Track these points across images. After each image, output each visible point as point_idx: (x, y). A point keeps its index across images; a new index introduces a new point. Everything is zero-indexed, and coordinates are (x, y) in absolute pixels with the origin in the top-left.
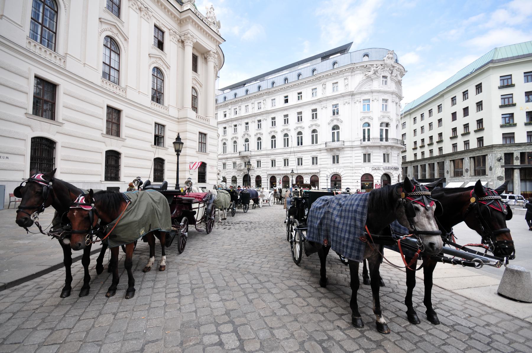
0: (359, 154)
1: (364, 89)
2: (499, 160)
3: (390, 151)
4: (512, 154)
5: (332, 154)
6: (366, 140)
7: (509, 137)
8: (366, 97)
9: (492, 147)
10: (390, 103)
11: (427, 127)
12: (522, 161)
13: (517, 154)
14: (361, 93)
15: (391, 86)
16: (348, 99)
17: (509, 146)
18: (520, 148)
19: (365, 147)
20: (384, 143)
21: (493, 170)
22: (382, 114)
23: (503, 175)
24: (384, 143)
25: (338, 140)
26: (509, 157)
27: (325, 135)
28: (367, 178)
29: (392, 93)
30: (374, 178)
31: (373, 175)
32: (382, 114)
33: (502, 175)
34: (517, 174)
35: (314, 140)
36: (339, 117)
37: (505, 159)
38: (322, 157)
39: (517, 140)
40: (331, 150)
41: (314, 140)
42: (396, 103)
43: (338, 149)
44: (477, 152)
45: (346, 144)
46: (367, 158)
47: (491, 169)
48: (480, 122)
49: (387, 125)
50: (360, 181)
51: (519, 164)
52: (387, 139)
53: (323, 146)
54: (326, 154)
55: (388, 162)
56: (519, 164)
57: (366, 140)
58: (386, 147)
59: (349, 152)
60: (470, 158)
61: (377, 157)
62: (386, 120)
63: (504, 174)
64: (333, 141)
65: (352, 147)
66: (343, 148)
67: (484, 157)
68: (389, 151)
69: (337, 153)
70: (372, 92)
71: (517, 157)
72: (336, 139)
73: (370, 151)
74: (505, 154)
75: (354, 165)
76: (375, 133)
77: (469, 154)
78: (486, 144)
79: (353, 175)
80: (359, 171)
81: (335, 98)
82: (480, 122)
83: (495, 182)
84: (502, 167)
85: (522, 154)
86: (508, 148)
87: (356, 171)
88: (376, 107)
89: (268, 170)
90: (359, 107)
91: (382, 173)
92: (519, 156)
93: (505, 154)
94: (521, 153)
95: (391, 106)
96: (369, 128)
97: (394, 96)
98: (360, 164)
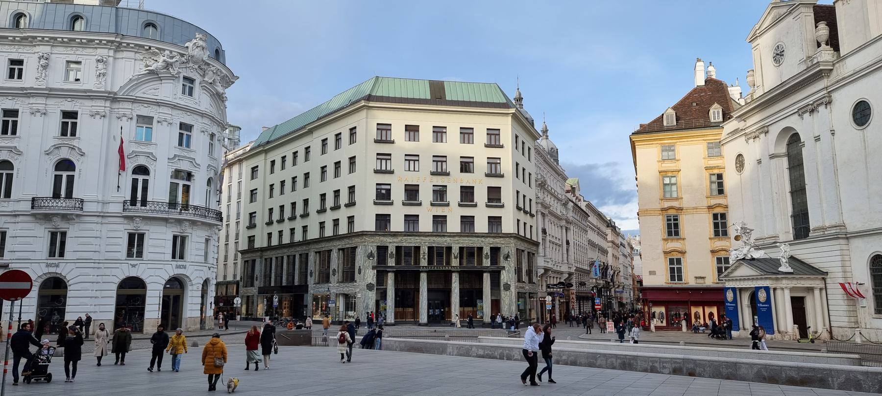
1: (139, 94)
2: (371, 255)
3: (189, 231)
5: (50, 226)
6: (139, 204)
7: (383, 220)
8: (145, 111)
9: (362, 234)
10: (195, 133)
11: (315, 176)
12: (398, 262)
13: (392, 249)
15: (202, 100)
17: (383, 235)
18: (395, 240)
19: (130, 218)
21: (362, 272)
22: (178, 152)
23: (374, 282)
25: (69, 195)
26: (382, 250)
29: (203, 115)
30: (149, 287)
31: (147, 281)
32: (178, 152)
36: (75, 143)
38: (19, 233)
40: (47, 217)
42: (212, 136)
43: (65, 217)
44: (347, 241)
46: (136, 243)
47: (360, 273)
48: (352, 189)
53: (26, 206)
54: (31, 225)
57: (139, 204)
58: (179, 222)
59: (93, 226)
60: (339, 249)
62: (185, 166)
63: (375, 279)
66: (78, 216)
67: (354, 249)
68: (188, 231)
69: (62, 225)
70: (158, 104)
72: (63, 193)
73: (143, 227)
74: (378, 247)
77: (338, 243)
78: (357, 228)
79: (99, 279)
82: (352, 189)
84: (374, 268)
85: (398, 249)
86: (382, 238)
87: (108, 272)
88: (165, 138)
93: (378, 247)
95: (199, 140)
96: (146, 177)
97: (206, 121)
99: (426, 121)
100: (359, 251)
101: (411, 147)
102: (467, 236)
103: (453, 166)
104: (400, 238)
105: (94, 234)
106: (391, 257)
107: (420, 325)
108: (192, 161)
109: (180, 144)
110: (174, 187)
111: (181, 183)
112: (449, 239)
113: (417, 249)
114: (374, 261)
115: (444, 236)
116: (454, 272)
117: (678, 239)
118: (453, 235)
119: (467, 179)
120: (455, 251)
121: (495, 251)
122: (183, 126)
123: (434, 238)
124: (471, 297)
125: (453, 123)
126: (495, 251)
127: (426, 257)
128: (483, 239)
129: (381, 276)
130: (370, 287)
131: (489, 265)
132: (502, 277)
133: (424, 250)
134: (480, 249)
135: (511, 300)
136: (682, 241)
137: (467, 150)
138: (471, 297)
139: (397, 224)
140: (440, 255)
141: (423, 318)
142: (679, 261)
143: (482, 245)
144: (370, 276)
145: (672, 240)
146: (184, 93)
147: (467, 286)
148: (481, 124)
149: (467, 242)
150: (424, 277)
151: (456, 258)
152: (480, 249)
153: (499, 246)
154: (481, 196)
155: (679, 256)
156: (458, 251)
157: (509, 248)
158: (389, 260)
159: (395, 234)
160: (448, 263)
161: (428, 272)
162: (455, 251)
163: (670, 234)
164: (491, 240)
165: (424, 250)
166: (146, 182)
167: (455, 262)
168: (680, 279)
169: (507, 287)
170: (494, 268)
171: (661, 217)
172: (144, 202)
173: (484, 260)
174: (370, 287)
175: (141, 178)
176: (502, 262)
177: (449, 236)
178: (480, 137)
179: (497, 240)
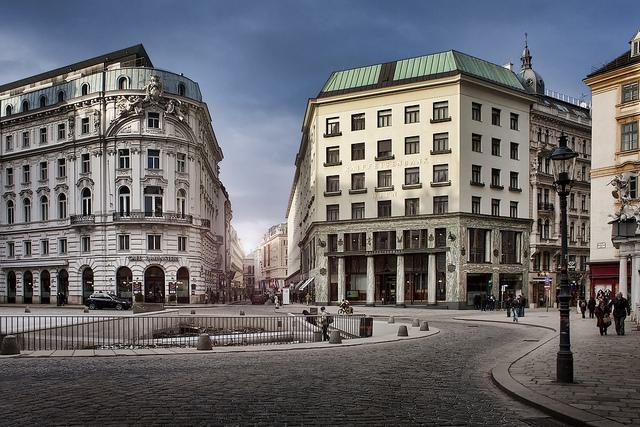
0: (112, 235)
12: (347, 248)
13: (341, 237)
14: (116, 140)
16: (96, 148)
17: (332, 225)
20: (153, 219)
23: (326, 267)
24: (153, 219)
26: (332, 237)
27: (74, 207)
28: (123, 274)
29: (167, 141)
35: (62, 208)
39: (342, 217)
41: (62, 208)
45: (98, 220)
46: (124, 243)
49: (158, 190)
50: (114, 278)
52: (159, 212)
55: (158, 247)
58: (151, 226)
61: (139, 242)
62: (153, 183)
64: (85, 214)
65: (104, 225)
75: (108, 253)
76: (137, 202)
80: (114, 263)
81: (86, 143)
85: (346, 236)
89: (4, 262)
90: (113, 160)
91: (144, 265)
94: (345, 234)
98: (114, 252)
99: (370, 109)
101: (358, 137)
105: (100, 238)
107: (368, 306)
108: (160, 178)
109: (150, 165)
110: (148, 201)
111: (154, 196)
114: (326, 249)
118: (398, 219)
119: (412, 160)
120: (400, 235)
121: (441, 232)
122: (151, 152)
124: (416, 278)
126: (441, 232)
130: (323, 272)
134: (425, 231)
137: (412, 130)
138: (416, 278)
139: (345, 214)
140: (384, 239)
141: (400, 297)
146: (150, 125)
147: (410, 269)
149: (411, 225)
151: (400, 241)
152: (425, 231)
153: (444, 226)
157: (455, 227)
159: (343, 223)
160: (394, 246)
161: (374, 256)
162: (400, 235)
164: (436, 221)
165: (370, 236)
166: (128, 198)
167: (400, 246)
169: (452, 268)
170: (438, 250)
172: (128, 214)
174: (323, 272)
175: (124, 196)
177: (393, 221)
179: (442, 221)
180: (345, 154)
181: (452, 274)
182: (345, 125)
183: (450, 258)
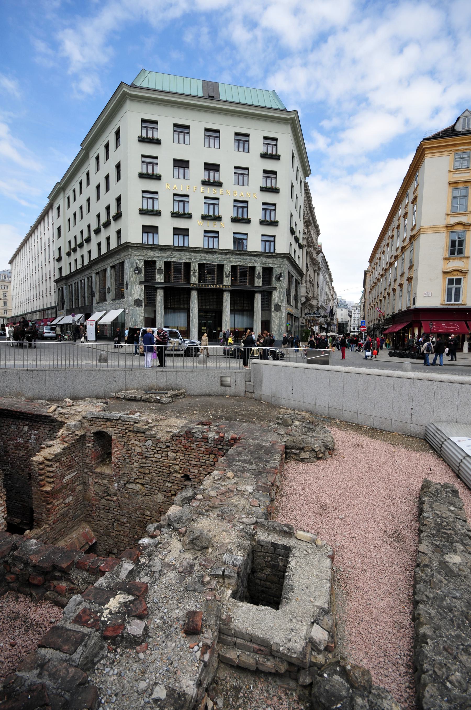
4: (155, 262)
12: (167, 277)
13: (160, 264)
18: (164, 255)
21: (129, 286)
33: (140, 298)
34: (160, 297)
37: (145, 271)
47: (127, 288)
51: (163, 281)
56: (163, 281)
63: (143, 295)
67: (122, 263)
71: (160, 268)
83: (131, 308)
84: (141, 283)
85: (167, 264)
86: (149, 252)
92: (163, 268)
99: (198, 124)
100: (127, 265)
102: (240, 254)
103: (226, 175)
104: (169, 253)
106: (160, 273)
112: (220, 256)
113: (188, 265)
115: (215, 253)
116: (225, 291)
117: (461, 258)
119: (241, 193)
120: (227, 269)
121: (268, 271)
123: (205, 255)
125: (228, 128)
126: (268, 271)
127: (197, 274)
128: (256, 258)
129: (150, 292)
130: (137, 303)
131: (261, 285)
132: (273, 298)
133: (195, 266)
135: (281, 321)
136: (465, 260)
137: (243, 159)
142: (459, 281)
143: (255, 264)
144: (136, 291)
145: (454, 259)
148: (257, 133)
149: (239, 261)
150: (194, 295)
151: (227, 276)
152: (253, 269)
153: (271, 266)
154: (255, 213)
155: (459, 276)
156: (229, 270)
158: (158, 275)
159: (163, 248)
160: (221, 281)
162: (227, 269)
163: (452, 253)
164: (263, 260)
165: (195, 266)
167: (227, 281)
168: (457, 299)
169: (278, 308)
170: (266, 289)
171: (445, 234)
173: (256, 280)
174: (137, 303)
176: (275, 283)
178: (257, 145)
179: (270, 260)
180: (165, 167)
181: (278, 313)
182: (165, 131)
183: (276, 297)
